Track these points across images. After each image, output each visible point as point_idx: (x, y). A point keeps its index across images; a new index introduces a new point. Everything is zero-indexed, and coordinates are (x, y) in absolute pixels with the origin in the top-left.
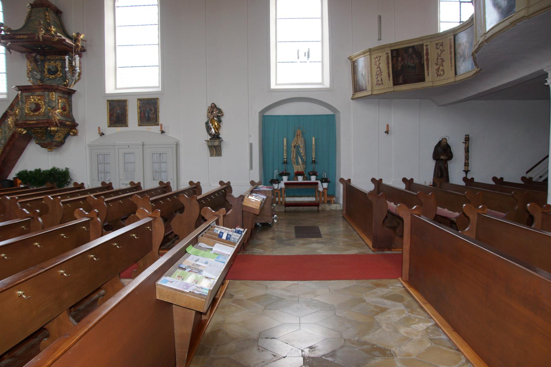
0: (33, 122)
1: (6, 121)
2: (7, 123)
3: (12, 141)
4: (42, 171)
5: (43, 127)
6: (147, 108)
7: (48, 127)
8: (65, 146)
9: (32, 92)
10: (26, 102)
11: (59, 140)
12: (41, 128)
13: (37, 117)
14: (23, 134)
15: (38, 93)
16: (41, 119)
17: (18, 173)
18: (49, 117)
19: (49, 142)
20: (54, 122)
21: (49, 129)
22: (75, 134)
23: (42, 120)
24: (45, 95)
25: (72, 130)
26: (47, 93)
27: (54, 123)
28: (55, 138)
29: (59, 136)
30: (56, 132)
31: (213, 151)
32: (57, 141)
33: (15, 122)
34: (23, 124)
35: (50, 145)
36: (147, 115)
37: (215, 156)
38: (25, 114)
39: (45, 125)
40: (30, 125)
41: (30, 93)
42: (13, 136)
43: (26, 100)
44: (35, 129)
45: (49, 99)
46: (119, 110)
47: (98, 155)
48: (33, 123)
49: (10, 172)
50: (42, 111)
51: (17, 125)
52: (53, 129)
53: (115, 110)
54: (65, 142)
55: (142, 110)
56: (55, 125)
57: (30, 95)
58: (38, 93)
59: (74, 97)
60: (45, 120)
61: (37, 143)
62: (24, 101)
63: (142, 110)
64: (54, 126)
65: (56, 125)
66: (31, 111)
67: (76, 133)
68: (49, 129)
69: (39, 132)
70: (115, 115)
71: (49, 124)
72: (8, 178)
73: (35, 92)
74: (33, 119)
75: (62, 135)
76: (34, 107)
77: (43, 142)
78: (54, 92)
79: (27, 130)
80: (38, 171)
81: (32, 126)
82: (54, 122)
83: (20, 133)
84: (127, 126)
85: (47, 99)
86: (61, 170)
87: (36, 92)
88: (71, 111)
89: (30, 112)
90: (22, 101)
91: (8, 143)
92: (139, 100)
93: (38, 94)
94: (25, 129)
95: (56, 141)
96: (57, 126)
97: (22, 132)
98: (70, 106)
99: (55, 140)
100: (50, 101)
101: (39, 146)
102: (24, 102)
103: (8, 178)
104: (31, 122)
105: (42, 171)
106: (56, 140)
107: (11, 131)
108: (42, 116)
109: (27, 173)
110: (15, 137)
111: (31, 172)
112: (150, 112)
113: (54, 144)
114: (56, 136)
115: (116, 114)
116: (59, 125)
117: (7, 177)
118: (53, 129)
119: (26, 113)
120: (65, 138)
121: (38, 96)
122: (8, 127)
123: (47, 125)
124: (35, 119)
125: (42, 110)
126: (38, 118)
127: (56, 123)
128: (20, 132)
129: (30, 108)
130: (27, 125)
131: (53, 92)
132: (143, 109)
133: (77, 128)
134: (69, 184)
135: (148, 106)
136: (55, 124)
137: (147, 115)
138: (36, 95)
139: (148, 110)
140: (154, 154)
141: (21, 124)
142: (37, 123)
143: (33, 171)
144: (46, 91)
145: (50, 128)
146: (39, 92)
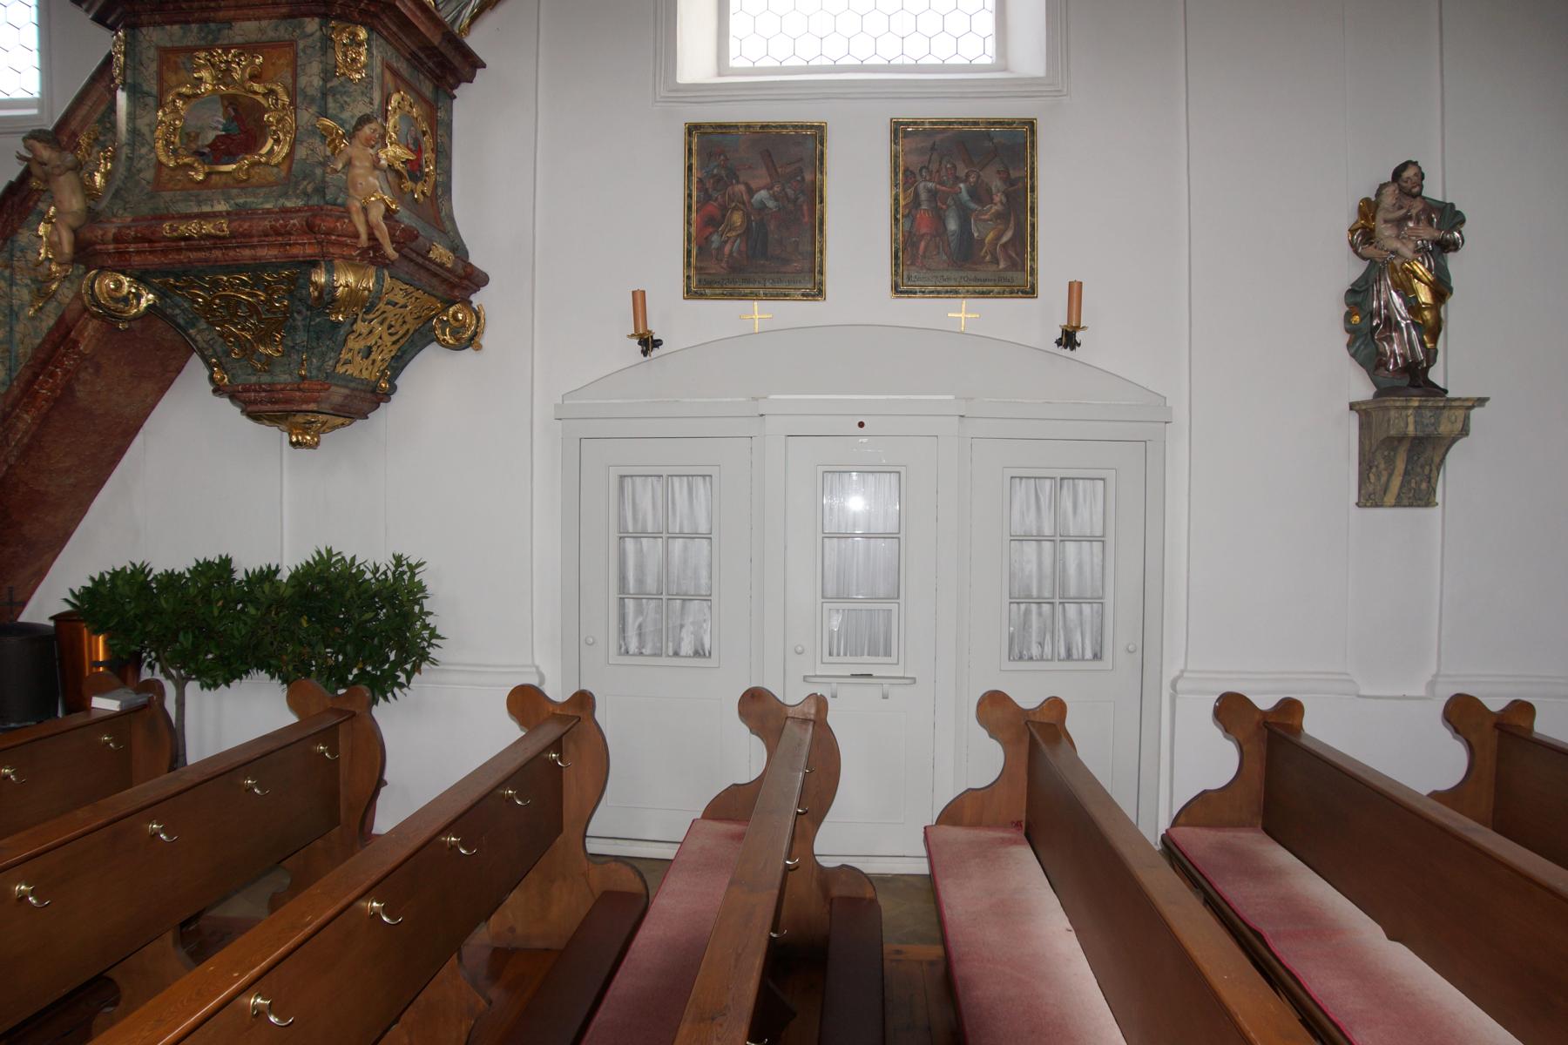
0: (208, 228)
1: (24, 237)
2: (31, 256)
3: (52, 375)
4: (239, 576)
5: (276, 267)
6: (957, 179)
7: (313, 264)
8: (385, 416)
9: (206, 21)
10: (162, 93)
11: (365, 375)
12: (257, 268)
13: (235, 191)
14: (135, 318)
15: (251, 25)
16: (268, 206)
17: (89, 584)
18: (321, 190)
19: (303, 378)
20: (362, 229)
21: (320, 278)
22: (467, 339)
23: (269, 212)
24: (301, 44)
25: (451, 311)
26: (312, 25)
27: (357, 236)
28: (345, 356)
29: (371, 341)
30: (364, 304)
31: (1390, 475)
32: (352, 379)
33: (75, 231)
34: (136, 240)
35: (307, 402)
36: (952, 225)
37: (1398, 504)
38: (149, 175)
39: (295, 251)
40: (179, 250)
41: (194, 27)
42: (63, 335)
43: (161, 79)
44: (216, 284)
45: (328, 74)
46: (769, 188)
47: (622, 477)
48: (209, 236)
49: (40, 574)
50: (271, 151)
51: (86, 254)
52: (346, 279)
53: (742, 187)
54: (394, 388)
55: (923, 196)
56: (364, 252)
57: (191, 40)
58: (247, 29)
59: (467, 103)
60: (299, 210)
61: (218, 390)
62: (152, 86)
63: (923, 196)
64: (351, 263)
65: (372, 256)
66: (199, 154)
67: (475, 334)
68: (320, 278)
69: (239, 302)
70: (737, 218)
71: (320, 243)
72: (25, 617)
73: (229, 23)
74: (206, 209)
75: (388, 340)
76: (214, 124)
77: (266, 378)
78: (363, 24)
79: (161, 293)
80: (216, 572)
81: (193, 255)
82: (362, 229)
83: (109, 316)
84: (818, 292)
85: (315, 67)
86: (368, 576)
87: (238, 26)
88: (443, 188)
89: (187, 160)
90: (134, 92)
91: (31, 383)
92: (899, 130)
93: (254, 37)
94: (141, 278)
95: (347, 380)
96: (373, 262)
97: (126, 300)
98: (443, 154)
99: (341, 370)
100: (335, 82)
101: (227, 409)
102: (149, 94)
103: (25, 617)
104: (192, 228)
105: (239, 576)
106: (351, 370)
107: (52, 306)
108: (270, 185)
109: (145, 586)
110: (76, 343)
111: (171, 579)
112: (973, 205)
113: (338, 394)
114: (351, 344)
115: (747, 216)
116: (389, 250)
117: (18, 617)
118: (346, 279)
119: (160, 164)
120: (399, 363)
121: (249, 48)
122: (35, 281)
123: (309, 251)
124: (221, 207)
125: (274, 149)
126: (241, 201)
127: (372, 237)
128: (112, 305)
129: (189, 136)
130: (164, 252)
131: (356, 24)
132: (930, 185)
133: (476, 299)
134: (424, 666)
135: (962, 171)
136: (364, 240)
137: (952, 225)
138: (239, 39)
139: (965, 196)
140: (1021, 478)
141: (117, 239)
142: (233, 235)
143: (181, 575)
144: (312, 15)
145: (330, 272)
146: (258, 19)
